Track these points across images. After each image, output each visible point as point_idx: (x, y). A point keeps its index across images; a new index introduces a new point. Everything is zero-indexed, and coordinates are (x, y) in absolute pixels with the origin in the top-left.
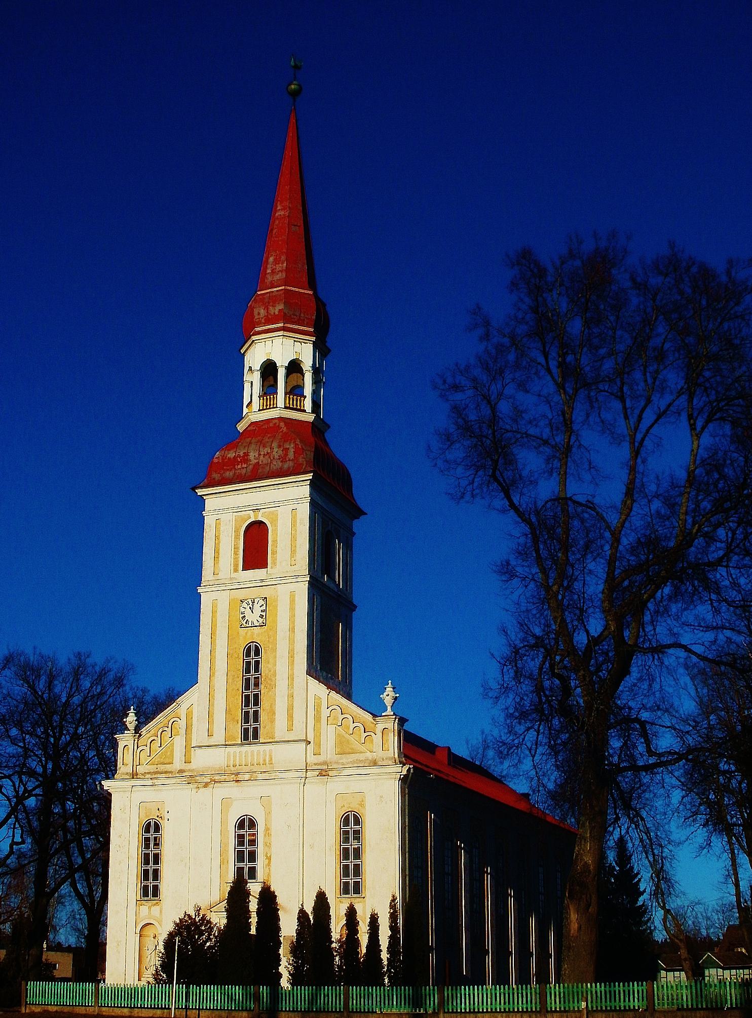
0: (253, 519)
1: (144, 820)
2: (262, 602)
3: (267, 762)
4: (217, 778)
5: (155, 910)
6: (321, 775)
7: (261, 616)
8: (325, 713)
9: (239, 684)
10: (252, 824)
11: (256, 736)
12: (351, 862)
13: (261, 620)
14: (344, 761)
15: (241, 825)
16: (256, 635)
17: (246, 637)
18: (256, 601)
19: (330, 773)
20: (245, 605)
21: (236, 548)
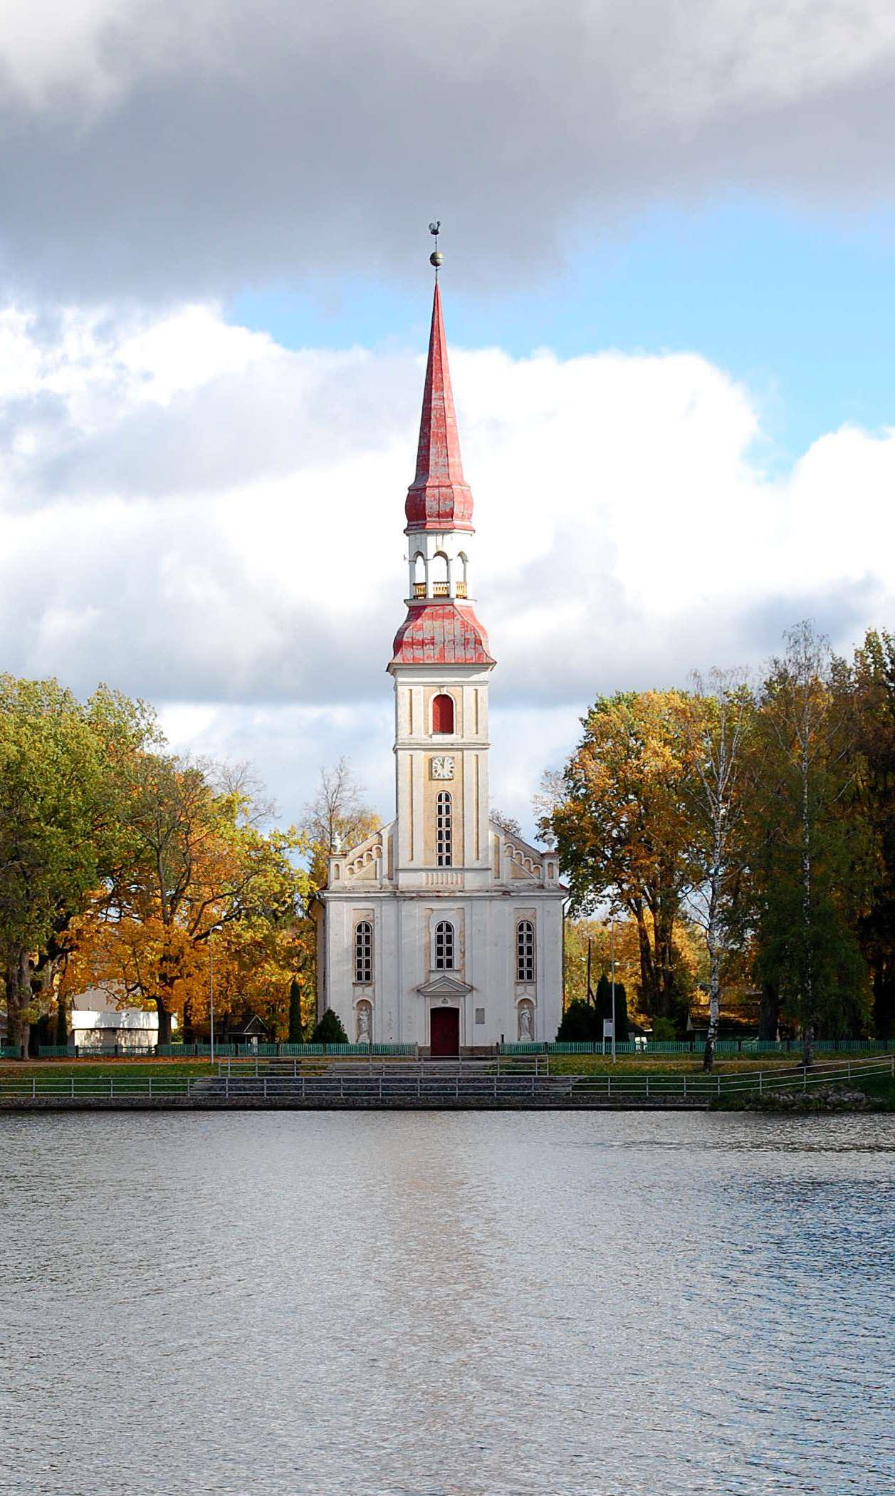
0: (438, 694)
1: (357, 922)
2: (451, 761)
3: (454, 882)
4: (422, 894)
5: (369, 990)
6: (503, 894)
7: (451, 772)
8: (503, 848)
9: (435, 822)
10: (449, 928)
11: (448, 862)
12: (525, 957)
13: (450, 774)
14: (518, 884)
15: (440, 929)
16: (446, 786)
17: (438, 787)
18: (446, 759)
19: (512, 894)
20: (436, 761)
21: (426, 715)
